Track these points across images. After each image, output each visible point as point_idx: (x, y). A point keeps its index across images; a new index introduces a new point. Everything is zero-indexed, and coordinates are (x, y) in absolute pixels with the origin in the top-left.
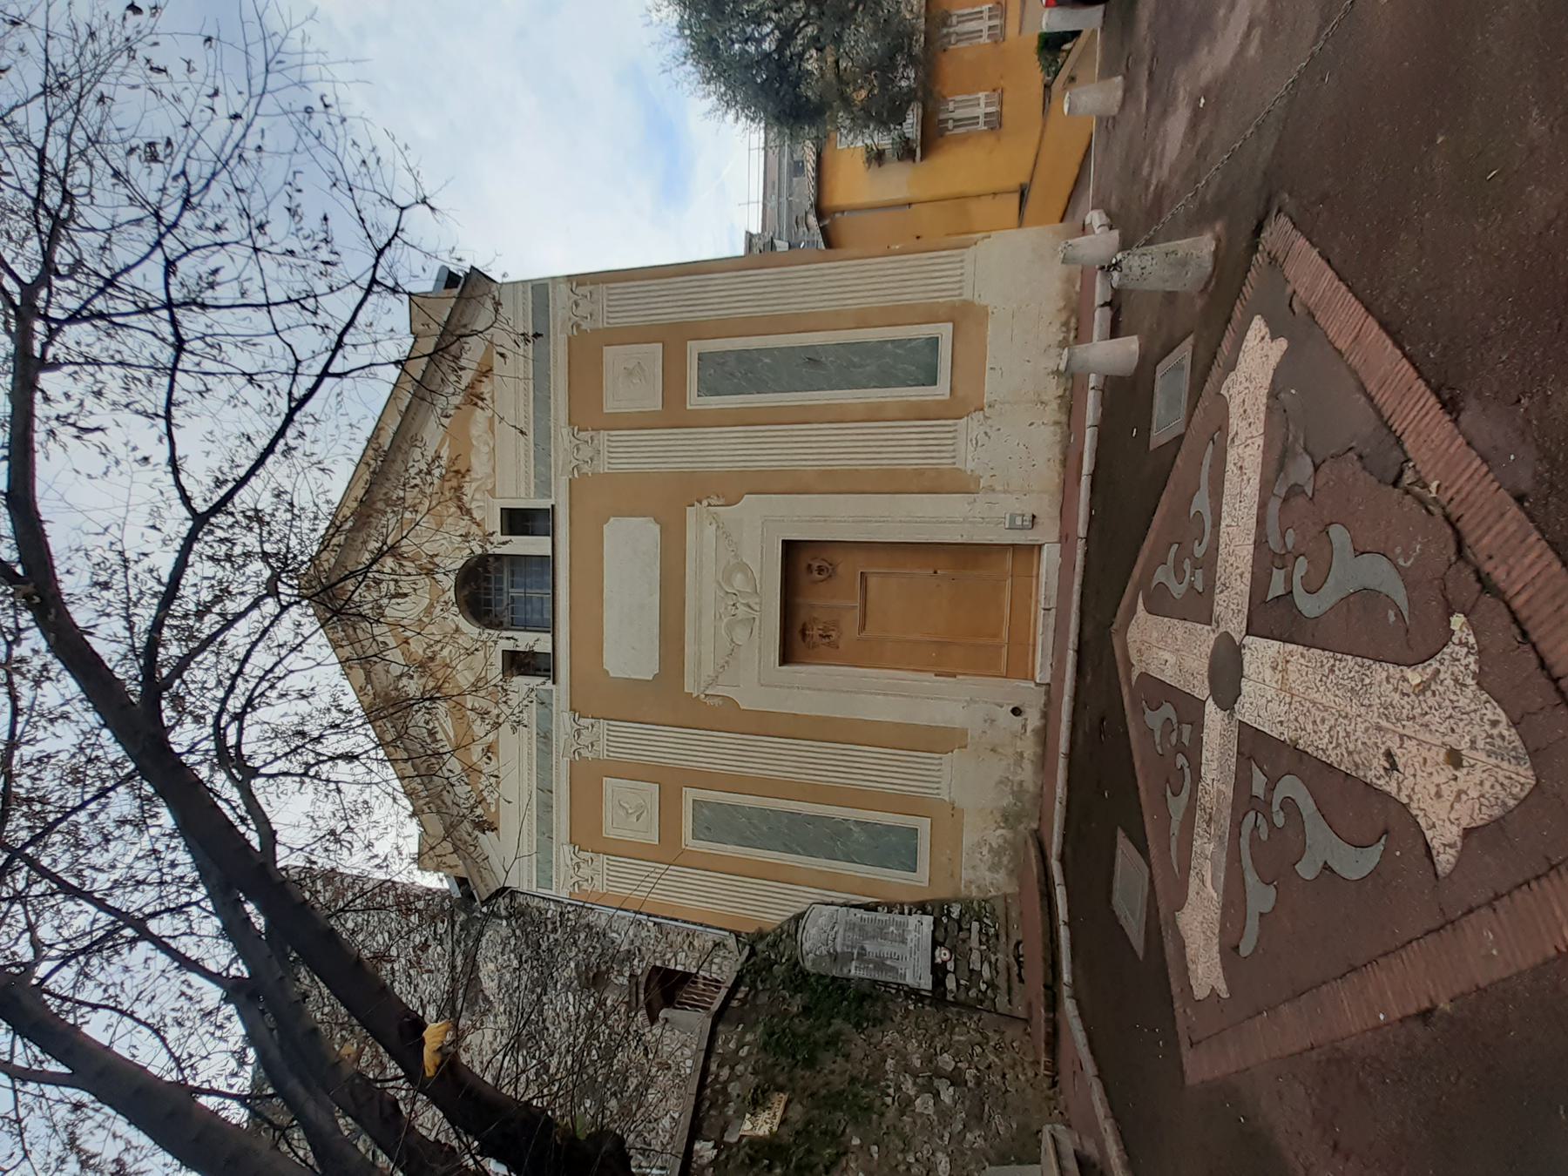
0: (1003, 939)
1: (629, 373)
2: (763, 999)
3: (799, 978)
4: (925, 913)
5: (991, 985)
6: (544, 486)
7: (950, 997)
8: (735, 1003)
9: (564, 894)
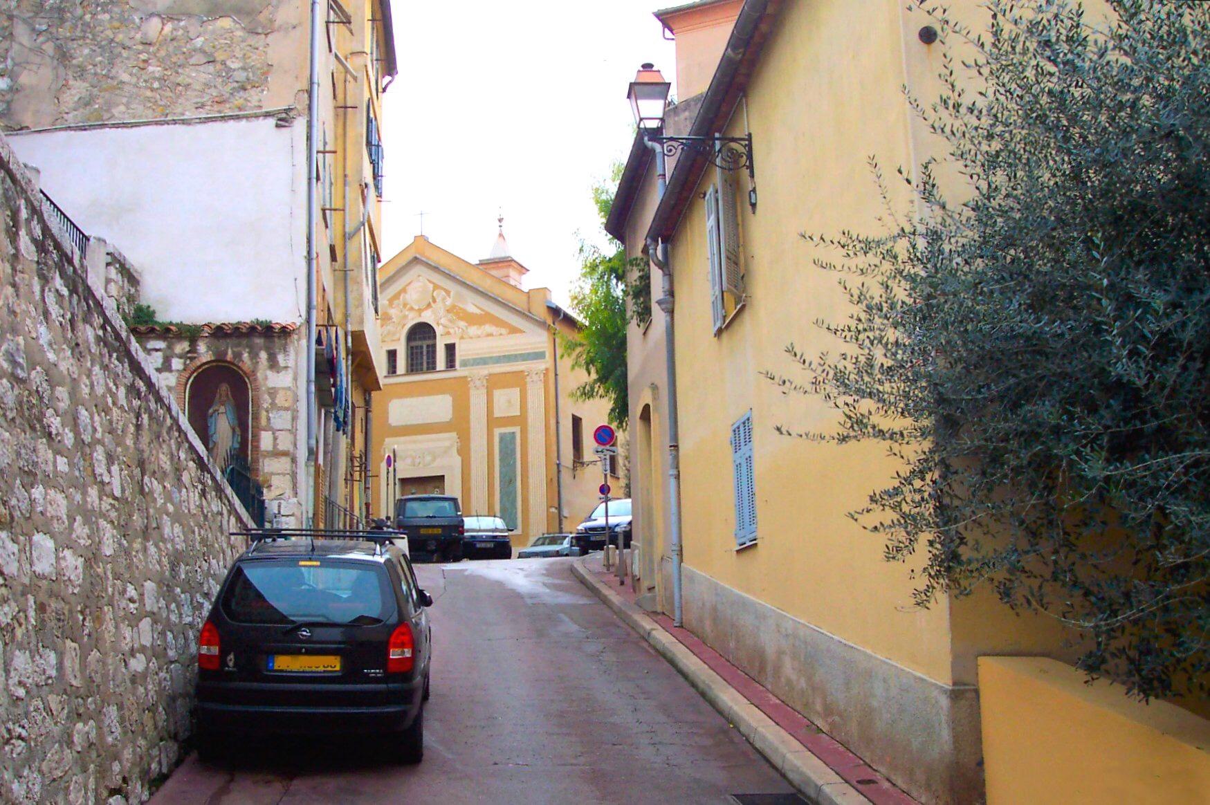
1: (509, 402)
6: (465, 364)
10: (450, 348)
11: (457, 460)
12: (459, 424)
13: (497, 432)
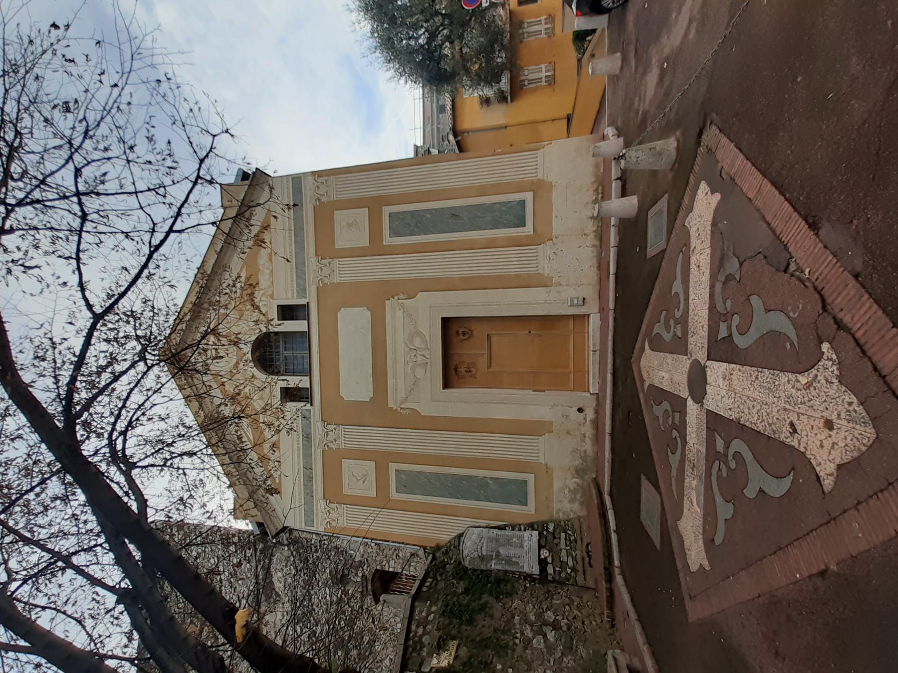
0: (579, 542)
1: (350, 225)
2: (441, 585)
3: (461, 572)
4: (533, 529)
5: (573, 569)
6: (302, 291)
7: (550, 578)
8: (424, 589)
9: (321, 529)
12: (377, 297)
13: (388, 240)
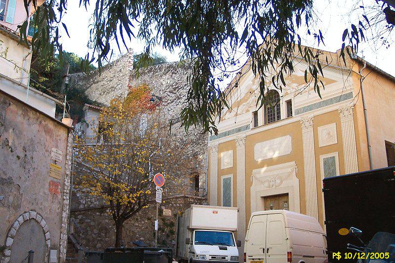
1: (329, 134)
9: (209, 145)
10: (289, 103)
11: (295, 182)
